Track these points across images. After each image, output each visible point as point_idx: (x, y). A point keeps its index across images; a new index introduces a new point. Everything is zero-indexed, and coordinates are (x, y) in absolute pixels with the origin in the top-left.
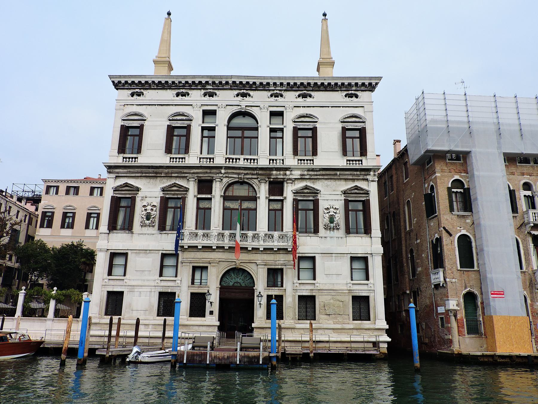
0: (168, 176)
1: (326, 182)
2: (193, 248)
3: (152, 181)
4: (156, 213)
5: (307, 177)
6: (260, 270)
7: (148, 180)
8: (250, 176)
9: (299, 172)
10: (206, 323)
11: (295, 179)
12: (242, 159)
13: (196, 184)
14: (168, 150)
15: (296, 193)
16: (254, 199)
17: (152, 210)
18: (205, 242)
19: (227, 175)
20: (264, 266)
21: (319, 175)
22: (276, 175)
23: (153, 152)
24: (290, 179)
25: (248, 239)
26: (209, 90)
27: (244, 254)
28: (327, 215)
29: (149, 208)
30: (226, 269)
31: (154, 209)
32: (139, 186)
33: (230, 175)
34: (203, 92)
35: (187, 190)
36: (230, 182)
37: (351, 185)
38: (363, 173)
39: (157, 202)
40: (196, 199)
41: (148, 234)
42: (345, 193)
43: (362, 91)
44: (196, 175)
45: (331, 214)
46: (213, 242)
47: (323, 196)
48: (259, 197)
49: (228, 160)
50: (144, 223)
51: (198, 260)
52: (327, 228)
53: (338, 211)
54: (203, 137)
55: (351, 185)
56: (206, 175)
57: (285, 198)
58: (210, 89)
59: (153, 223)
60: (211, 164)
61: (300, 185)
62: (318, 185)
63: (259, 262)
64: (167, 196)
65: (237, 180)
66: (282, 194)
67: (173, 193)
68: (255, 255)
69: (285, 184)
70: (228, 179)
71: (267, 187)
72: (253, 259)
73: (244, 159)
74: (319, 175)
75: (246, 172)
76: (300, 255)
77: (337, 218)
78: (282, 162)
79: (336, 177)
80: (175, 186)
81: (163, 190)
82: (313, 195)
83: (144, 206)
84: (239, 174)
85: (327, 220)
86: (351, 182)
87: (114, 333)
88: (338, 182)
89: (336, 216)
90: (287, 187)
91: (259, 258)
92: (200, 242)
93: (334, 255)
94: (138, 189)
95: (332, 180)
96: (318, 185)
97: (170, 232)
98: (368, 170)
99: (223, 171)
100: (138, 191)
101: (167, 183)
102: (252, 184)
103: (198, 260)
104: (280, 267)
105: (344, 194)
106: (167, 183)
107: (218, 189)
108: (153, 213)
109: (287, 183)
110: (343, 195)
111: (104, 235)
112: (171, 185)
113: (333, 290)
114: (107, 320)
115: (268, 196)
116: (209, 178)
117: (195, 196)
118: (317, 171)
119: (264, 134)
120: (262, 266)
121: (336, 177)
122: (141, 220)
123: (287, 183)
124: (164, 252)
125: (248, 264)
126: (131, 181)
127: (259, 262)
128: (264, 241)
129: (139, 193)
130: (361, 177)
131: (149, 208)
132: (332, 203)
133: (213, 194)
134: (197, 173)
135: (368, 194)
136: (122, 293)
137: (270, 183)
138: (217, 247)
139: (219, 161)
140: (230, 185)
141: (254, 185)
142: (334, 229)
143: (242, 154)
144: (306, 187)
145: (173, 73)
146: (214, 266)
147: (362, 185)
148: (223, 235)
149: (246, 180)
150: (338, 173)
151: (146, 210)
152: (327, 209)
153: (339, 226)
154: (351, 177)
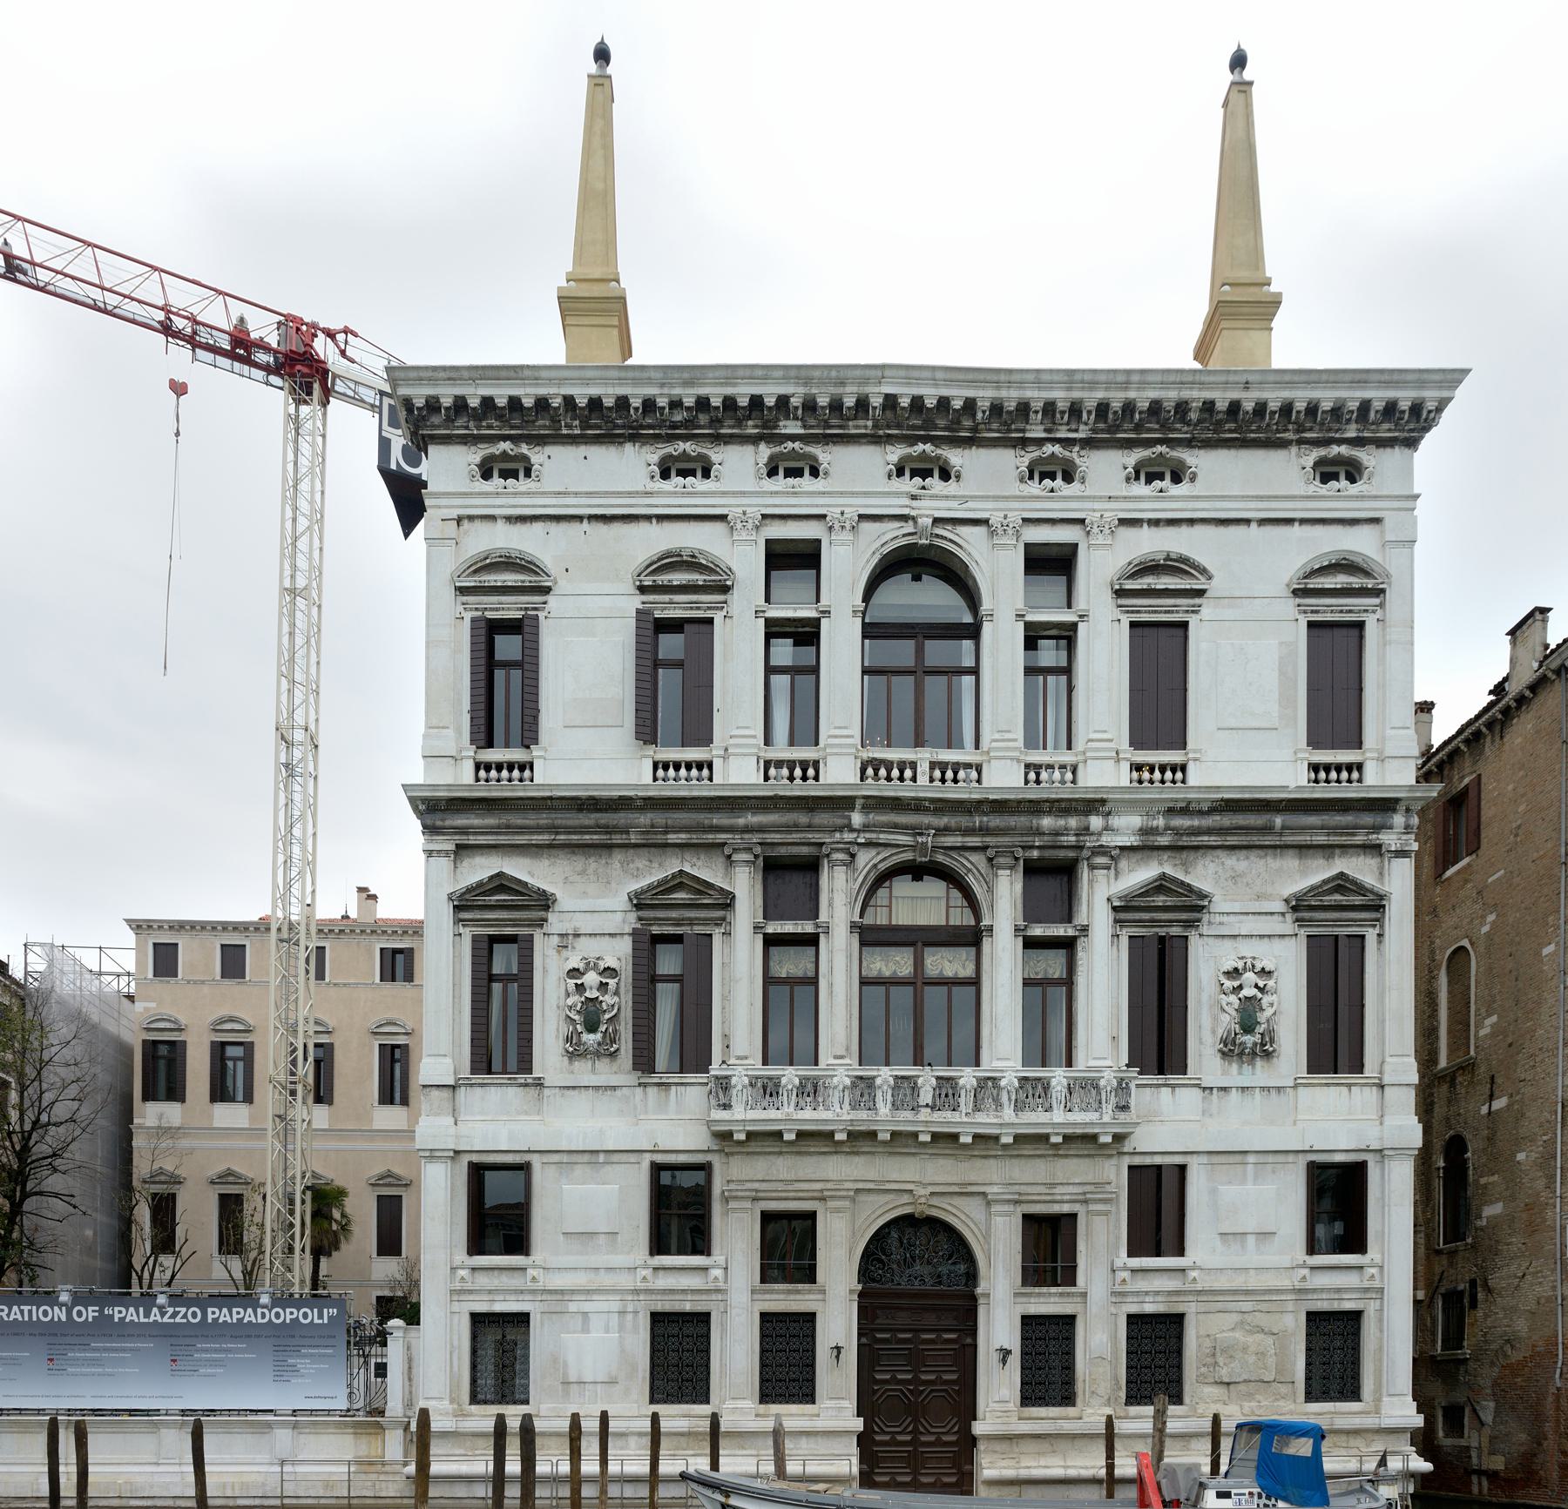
0: (655, 846)
1: (1234, 862)
2: (765, 1139)
3: (593, 864)
4: (618, 1001)
5: (1164, 840)
6: (999, 1221)
7: (578, 862)
8: (950, 841)
9: (1136, 821)
10: (820, 1424)
11: (1122, 848)
12: (923, 768)
13: (759, 877)
14: (647, 731)
15: (1124, 909)
16: (972, 938)
17: (603, 987)
18: (807, 1114)
19: (874, 836)
20: (1011, 1208)
21: (1209, 831)
22: (1057, 833)
23: (587, 742)
24: (1102, 850)
25: (962, 1100)
26: (790, 445)
27: (941, 1161)
28: (1233, 998)
29: (591, 978)
30: (881, 1222)
31: (612, 982)
32: (549, 889)
33: (883, 838)
34: (765, 451)
35: (727, 902)
36: (882, 867)
37: (1319, 872)
38: (1368, 819)
39: (618, 953)
40: (759, 939)
41: (597, 1088)
42: (1299, 906)
43: (1382, 443)
44: (756, 838)
45: (1248, 992)
46: (835, 1113)
47: (1218, 918)
48: (990, 929)
49: (870, 771)
50: (579, 1043)
51: (780, 1186)
52: (1231, 1050)
53: (1271, 983)
54: (770, 670)
55: (1319, 872)
56: (795, 837)
57: (1085, 930)
58: (793, 438)
59: (613, 1041)
60: (810, 790)
61: (1138, 875)
62: (1204, 875)
63: (995, 1189)
64: (656, 930)
65: (908, 856)
66: (1068, 918)
67: (674, 914)
68: (979, 1163)
69: (1084, 873)
70: (873, 852)
71: (1019, 887)
72: (973, 1178)
73: (933, 765)
74: (1209, 831)
75: (944, 821)
76: (1137, 1161)
77: (1269, 1012)
78: (1069, 776)
79: (1268, 840)
80: (680, 886)
81: (639, 902)
82: (1184, 916)
83: (574, 973)
84: (916, 830)
85: (1228, 1021)
86: (1322, 861)
87: (513, 1467)
88: (1274, 863)
89: (1266, 1000)
90: (1091, 882)
91: (993, 1174)
92: (789, 1115)
93: (1251, 1159)
94: (544, 902)
95: (1253, 854)
96: (1204, 875)
97: (675, 1078)
98: (1385, 805)
99: (857, 819)
100: (547, 908)
101: (652, 872)
102: (962, 871)
103: (780, 1186)
104: (1066, 1208)
105: (1295, 909)
106: (652, 872)
107: (838, 894)
108: (608, 999)
109: (1092, 867)
110: (1289, 917)
111: (435, 1093)
112: (660, 883)
113: (1247, 1292)
114: (483, 1418)
115: (1021, 923)
116: (805, 850)
117: (757, 928)
118: (1201, 813)
119: (1002, 647)
120: (1006, 1208)
121: (1268, 840)
122: (565, 1029)
123: (1092, 867)
124: (659, 1158)
125: (957, 1201)
126: (518, 868)
127: (995, 1189)
128: (1019, 1107)
129: (551, 917)
130: (1359, 839)
131: (591, 978)
132: (1248, 949)
133: (823, 917)
134: (761, 829)
135: (1379, 908)
136: (522, 1319)
137: (1032, 870)
138: (850, 1134)
139: (839, 773)
140: (884, 878)
141: (970, 879)
142: (1254, 1054)
143: (919, 742)
144: (1162, 885)
145: (629, 362)
146: (837, 1210)
147: (1360, 869)
148: (869, 1082)
149: (940, 858)
150: (1278, 821)
151: (580, 988)
152: (1234, 973)
153: (1272, 1041)
154: (1321, 839)
